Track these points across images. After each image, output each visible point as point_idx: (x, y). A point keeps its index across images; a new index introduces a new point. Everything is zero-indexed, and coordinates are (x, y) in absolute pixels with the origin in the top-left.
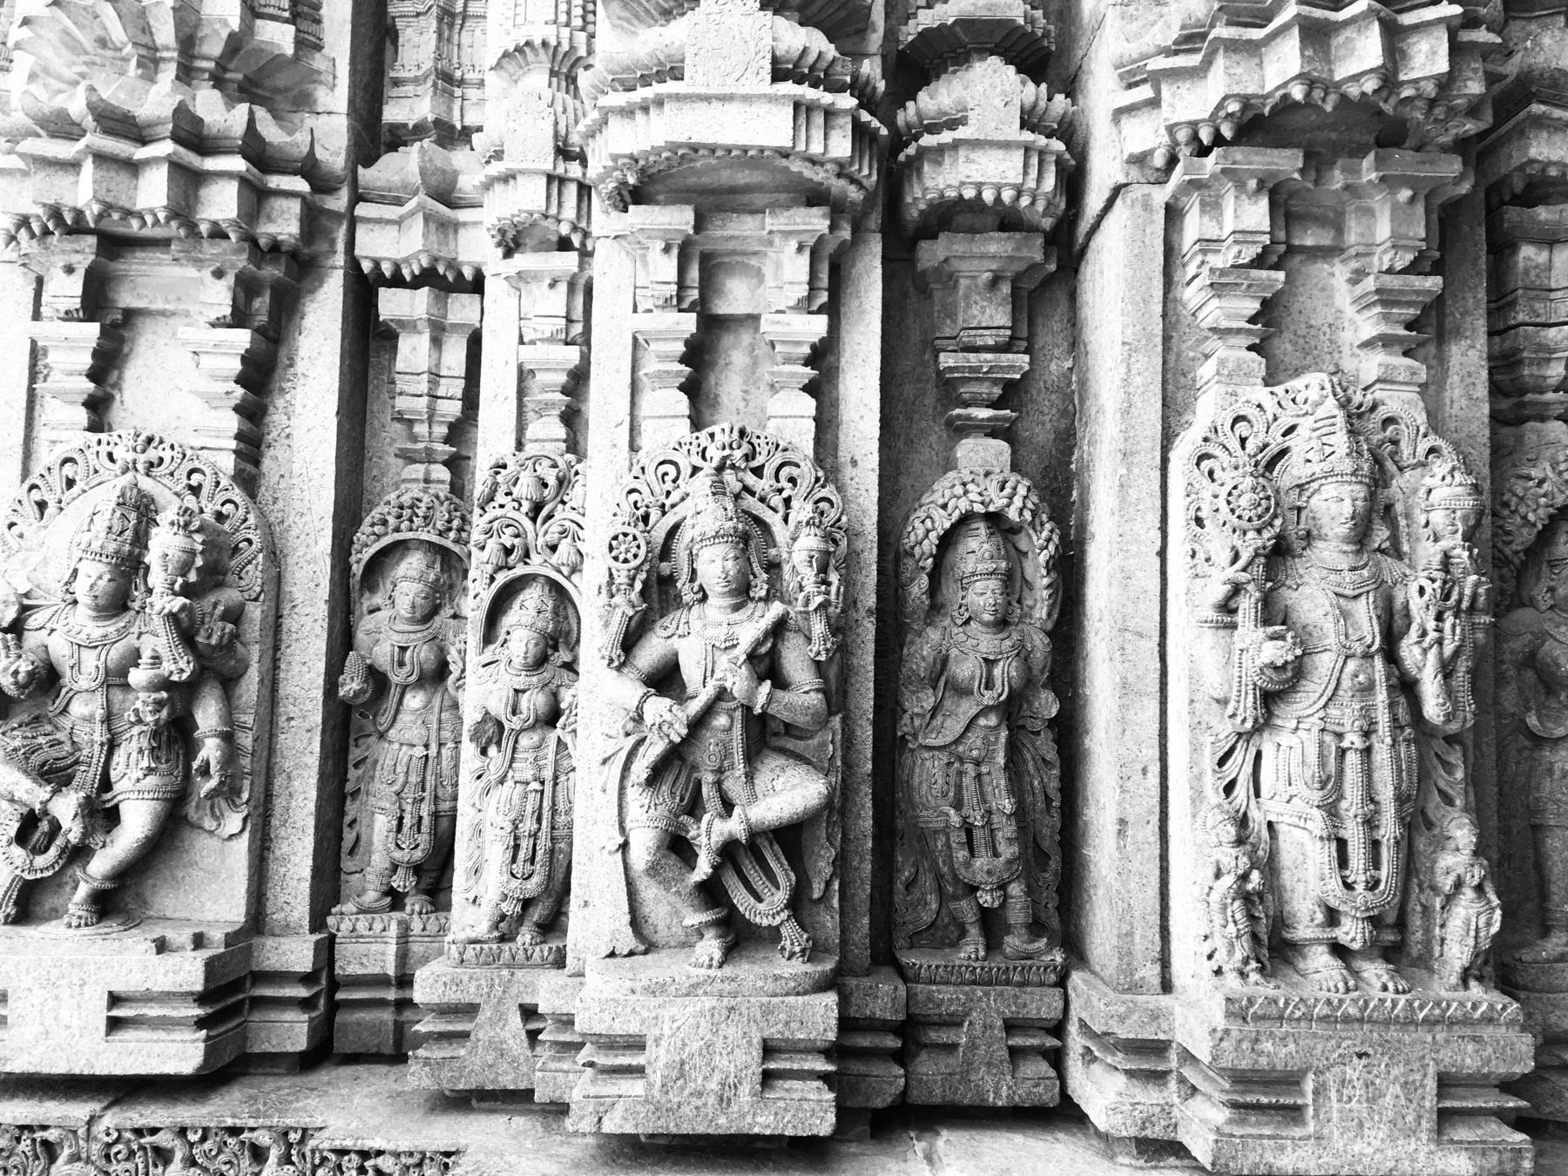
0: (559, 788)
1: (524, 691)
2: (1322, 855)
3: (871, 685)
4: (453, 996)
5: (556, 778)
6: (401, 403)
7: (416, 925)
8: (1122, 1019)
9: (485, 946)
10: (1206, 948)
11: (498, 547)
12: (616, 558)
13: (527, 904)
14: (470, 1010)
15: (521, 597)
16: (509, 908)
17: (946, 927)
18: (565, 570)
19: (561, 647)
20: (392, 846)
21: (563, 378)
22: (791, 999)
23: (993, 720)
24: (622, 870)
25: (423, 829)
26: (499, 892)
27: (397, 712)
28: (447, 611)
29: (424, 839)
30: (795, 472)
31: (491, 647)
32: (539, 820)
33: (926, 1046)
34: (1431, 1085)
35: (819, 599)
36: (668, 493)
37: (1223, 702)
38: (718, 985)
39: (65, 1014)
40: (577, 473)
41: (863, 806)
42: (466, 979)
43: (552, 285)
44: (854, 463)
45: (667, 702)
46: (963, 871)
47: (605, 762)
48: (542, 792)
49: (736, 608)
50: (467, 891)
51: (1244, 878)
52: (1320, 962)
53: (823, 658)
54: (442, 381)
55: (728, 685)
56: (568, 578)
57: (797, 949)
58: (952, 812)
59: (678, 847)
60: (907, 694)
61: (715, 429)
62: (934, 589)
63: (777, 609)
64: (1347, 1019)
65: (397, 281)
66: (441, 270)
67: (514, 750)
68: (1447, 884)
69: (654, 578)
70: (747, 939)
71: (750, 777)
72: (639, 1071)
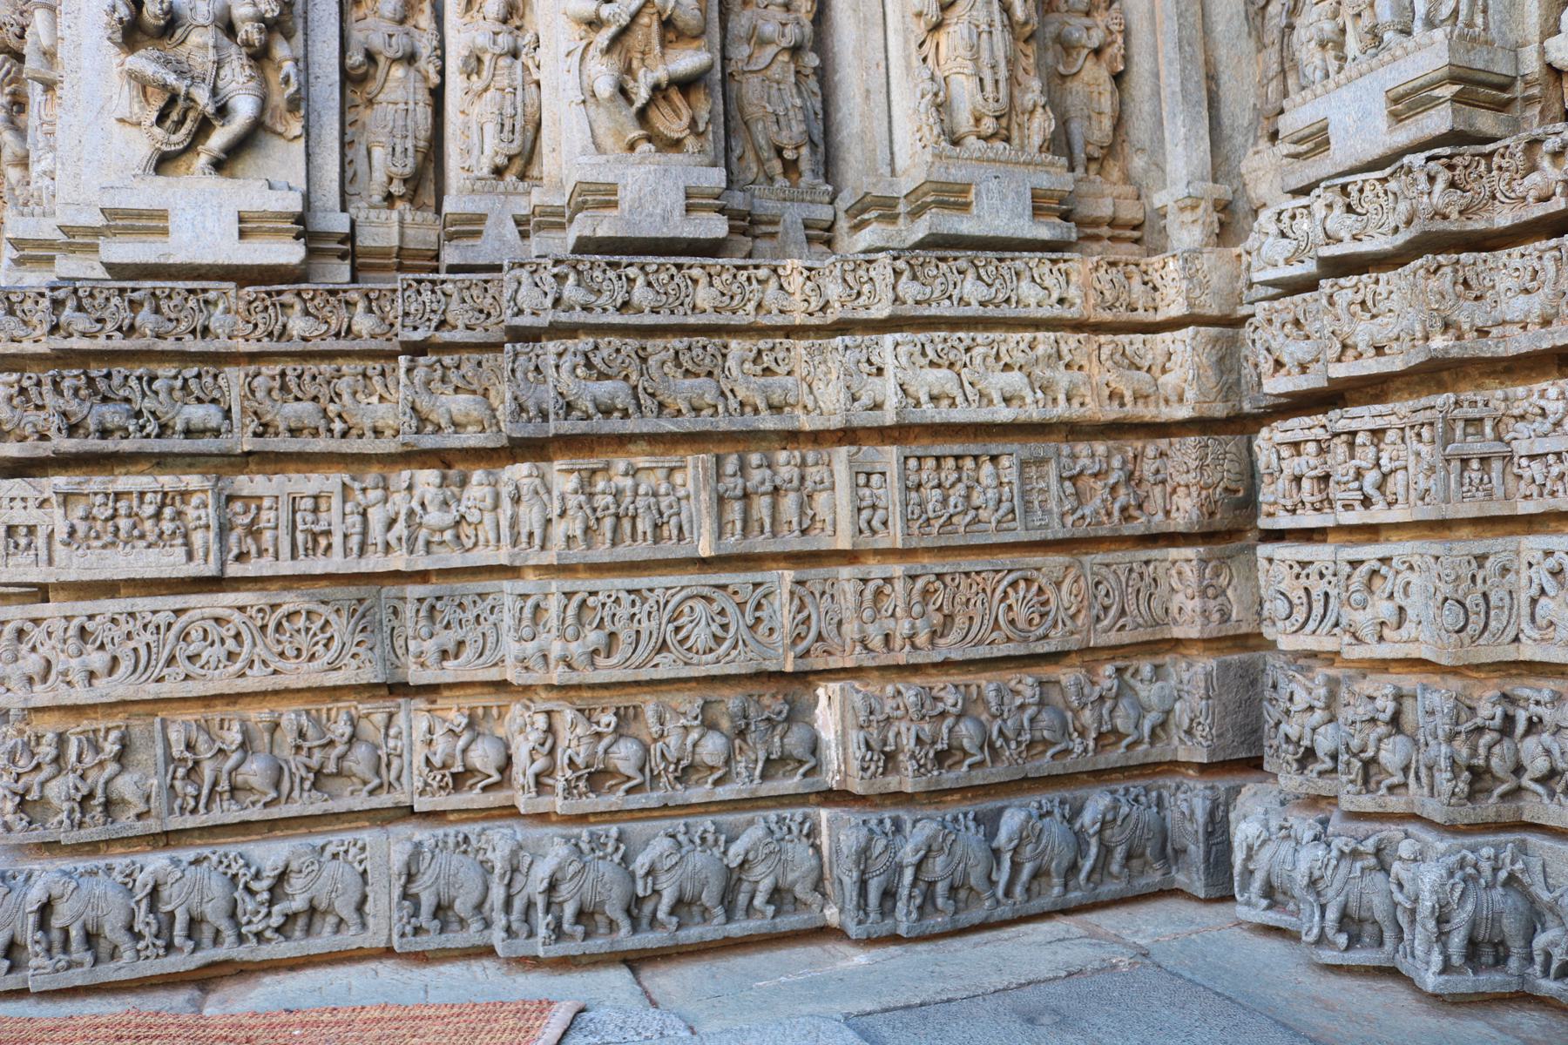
2: (972, 84)
7: (408, 217)
8: (875, 185)
10: (918, 136)
13: (510, 158)
14: (481, 218)
16: (501, 160)
23: (785, 57)
28: (411, 22)
29: (410, 162)
34: (1029, 194)
37: (919, 15)
39: (209, 224)
51: (936, 95)
52: (971, 140)
59: (623, 91)
64: (989, 160)
68: (1030, 106)
71: (663, 55)
72: (614, 205)
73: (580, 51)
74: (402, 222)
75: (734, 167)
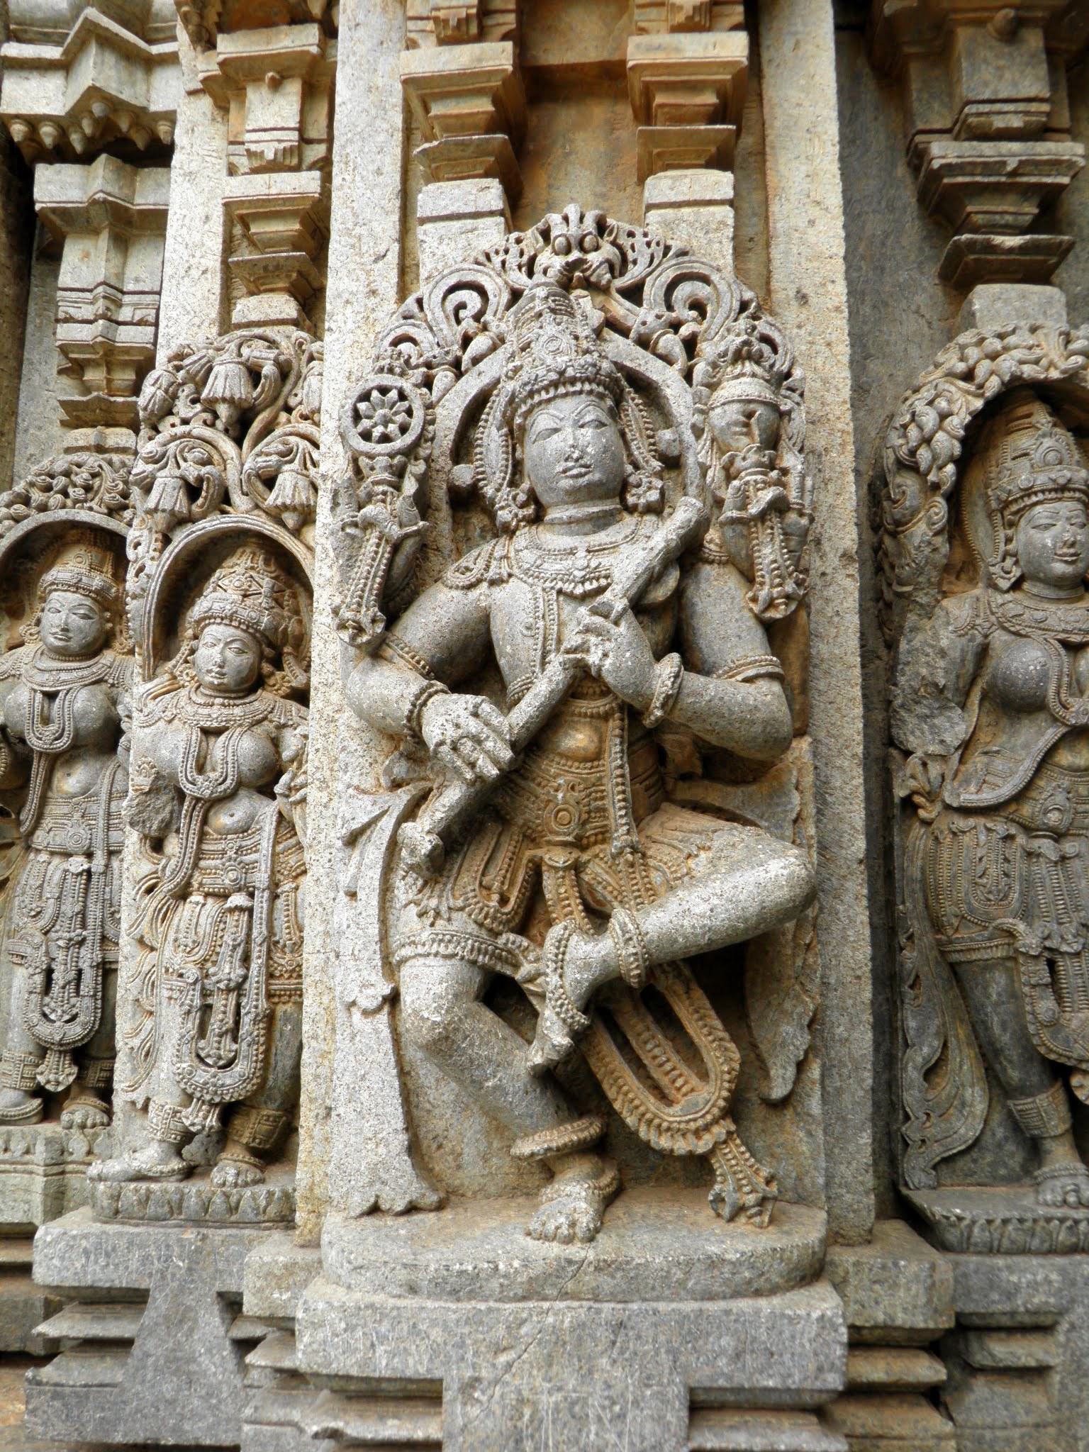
0: (280, 903)
1: (218, 732)
3: (857, 692)
4: (100, 1275)
5: (274, 885)
6: (67, 333)
9: (154, 1186)
11: (173, 482)
12: (366, 436)
13: (229, 1112)
15: (217, 574)
17: (1000, 1146)
18: (290, 519)
19: (289, 661)
20: (36, 1017)
21: (293, 227)
22: (744, 1305)
24: (389, 1046)
25: (84, 990)
26: (176, 1091)
27: (44, 801)
29: (86, 1007)
30: (702, 290)
31: (170, 664)
32: (246, 959)
33: (983, 1370)
35: (768, 495)
36: (466, 340)
38: (589, 1279)
40: (311, 358)
41: (851, 921)
42: (123, 1244)
43: (276, 85)
44: (803, 298)
45: (470, 699)
46: (1045, 1035)
47: (352, 840)
48: (250, 911)
49: (601, 522)
50: (133, 1088)
53: (777, 614)
54: (127, 299)
55: (593, 658)
56: (296, 533)
57: (751, 1199)
58: (1021, 927)
60: (911, 721)
61: (555, 218)
62: (955, 527)
63: (684, 513)
65: (61, 154)
66: (124, 125)
67: (202, 836)
69: (440, 495)
70: (638, 1180)
73: (388, 823)
74: (59, 1164)
75: (911, 1097)
